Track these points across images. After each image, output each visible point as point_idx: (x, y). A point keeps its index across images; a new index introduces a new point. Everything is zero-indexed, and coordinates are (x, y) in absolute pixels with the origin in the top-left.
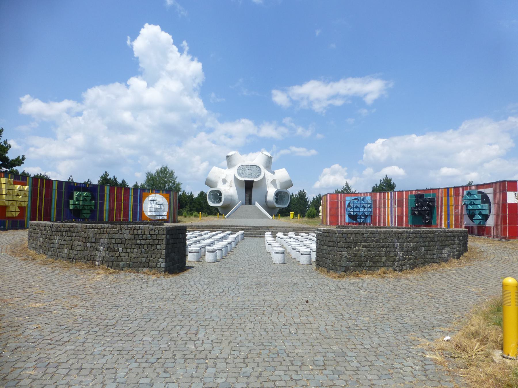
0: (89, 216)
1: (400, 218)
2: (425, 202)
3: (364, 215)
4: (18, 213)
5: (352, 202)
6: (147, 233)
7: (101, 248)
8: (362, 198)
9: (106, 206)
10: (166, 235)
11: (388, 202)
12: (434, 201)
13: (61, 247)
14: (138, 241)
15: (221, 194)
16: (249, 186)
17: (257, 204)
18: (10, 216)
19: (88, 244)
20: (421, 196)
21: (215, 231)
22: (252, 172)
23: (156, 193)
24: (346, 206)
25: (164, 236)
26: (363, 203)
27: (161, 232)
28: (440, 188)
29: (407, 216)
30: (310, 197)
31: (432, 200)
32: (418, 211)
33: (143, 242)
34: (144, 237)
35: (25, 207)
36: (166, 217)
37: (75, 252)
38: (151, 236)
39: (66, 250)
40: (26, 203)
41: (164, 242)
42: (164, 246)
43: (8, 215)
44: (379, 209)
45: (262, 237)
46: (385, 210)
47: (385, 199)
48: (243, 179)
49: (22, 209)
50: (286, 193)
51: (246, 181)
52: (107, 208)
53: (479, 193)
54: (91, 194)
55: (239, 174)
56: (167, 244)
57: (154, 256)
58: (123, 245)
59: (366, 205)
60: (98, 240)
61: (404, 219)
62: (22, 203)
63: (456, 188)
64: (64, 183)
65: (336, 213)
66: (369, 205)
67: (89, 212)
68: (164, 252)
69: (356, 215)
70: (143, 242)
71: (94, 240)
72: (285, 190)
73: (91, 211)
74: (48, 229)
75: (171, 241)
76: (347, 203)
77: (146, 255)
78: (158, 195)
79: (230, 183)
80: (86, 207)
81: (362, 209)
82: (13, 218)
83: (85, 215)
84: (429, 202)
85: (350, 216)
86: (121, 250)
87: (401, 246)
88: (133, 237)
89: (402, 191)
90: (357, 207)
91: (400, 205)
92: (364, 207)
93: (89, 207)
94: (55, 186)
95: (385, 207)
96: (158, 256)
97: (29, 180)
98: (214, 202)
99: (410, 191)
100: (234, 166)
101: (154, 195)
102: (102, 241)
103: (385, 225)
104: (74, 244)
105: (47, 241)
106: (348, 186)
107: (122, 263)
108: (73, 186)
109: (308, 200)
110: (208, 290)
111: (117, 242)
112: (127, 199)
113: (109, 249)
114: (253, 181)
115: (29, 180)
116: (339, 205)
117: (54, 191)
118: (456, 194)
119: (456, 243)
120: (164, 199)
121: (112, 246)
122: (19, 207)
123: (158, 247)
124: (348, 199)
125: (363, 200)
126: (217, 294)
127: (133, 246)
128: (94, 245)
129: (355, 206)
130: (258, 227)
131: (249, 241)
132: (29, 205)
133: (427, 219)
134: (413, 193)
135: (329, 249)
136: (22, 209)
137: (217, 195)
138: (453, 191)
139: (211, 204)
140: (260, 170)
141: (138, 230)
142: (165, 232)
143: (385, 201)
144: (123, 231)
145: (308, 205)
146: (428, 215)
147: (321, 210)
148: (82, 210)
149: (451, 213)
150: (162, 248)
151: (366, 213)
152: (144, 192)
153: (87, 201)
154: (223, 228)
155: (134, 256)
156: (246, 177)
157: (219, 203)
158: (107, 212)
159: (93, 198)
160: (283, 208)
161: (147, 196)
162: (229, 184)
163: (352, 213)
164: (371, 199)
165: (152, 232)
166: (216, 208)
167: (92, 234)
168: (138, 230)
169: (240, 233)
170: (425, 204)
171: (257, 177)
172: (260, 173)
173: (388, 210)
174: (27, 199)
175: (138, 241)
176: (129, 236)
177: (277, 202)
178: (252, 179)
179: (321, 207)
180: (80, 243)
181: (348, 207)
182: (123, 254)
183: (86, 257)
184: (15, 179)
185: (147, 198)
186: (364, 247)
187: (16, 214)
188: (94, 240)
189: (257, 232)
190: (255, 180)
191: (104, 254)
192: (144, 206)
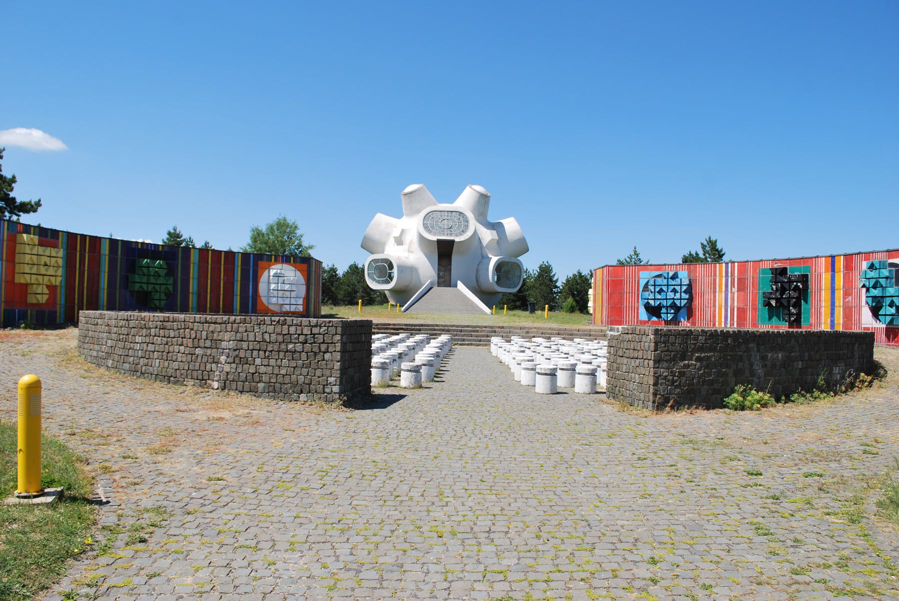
0: (163, 303)
1: (742, 312)
2: (790, 282)
3: (673, 306)
4: (46, 297)
5: (652, 282)
6: (306, 331)
7: (223, 358)
8: (671, 274)
9: (193, 286)
10: (342, 335)
11: (721, 281)
12: (807, 281)
13: (147, 355)
14: (290, 346)
15: (391, 266)
16: (444, 252)
17: (461, 286)
18: (34, 301)
19: (198, 351)
20: (783, 271)
21: (398, 334)
22: (451, 224)
23: (282, 262)
24: (641, 289)
25: (338, 337)
26: (673, 283)
27: (332, 330)
28: (818, 257)
29: (754, 309)
30: (561, 276)
31: (804, 279)
32: (777, 300)
33: (299, 347)
34: (302, 338)
35: (56, 286)
36: (301, 308)
37: (175, 365)
38: (314, 337)
39: (158, 361)
40: (59, 279)
41: (338, 349)
42: (338, 356)
43: (31, 299)
44: (702, 295)
45: (486, 345)
46: (715, 296)
47: (715, 275)
48: (435, 238)
49: (52, 288)
50: (518, 266)
52: (196, 289)
53: (891, 265)
54: (167, 264)
55: (426, 227)
56: (343, 352)
57: (318, 373)
58: (262, 353)
59: (678, 288)
60: (216, 343)
61: (749, 315)
62: (52, 279)
63: (848, 258)
64: (120, 243)
65: (622, 303)
66: (684, 288)
67: (163, 297)
68: (337, 365)
69: (660, 307)
70: (299, 347)
71: (208, 343)
72: (513, 260)
73: (166, 294)
74: (122, 323)
75: (349, 347)
76: (642, 283)
77: (305, 371)
78: (285, 266)
79: (409, 247)
80: (157, 287)
81: (671, 295)
82: (38, 305)
83: (157, 303)
84: (797, 282)
85: (648, 307)
86: (258, 361)
87: (764, 358)
88: (280, 338)
89: (747, 262)
90: (660, 292)
91: (742, 287)
92: (674, 291)
93: (163, 287)
94: (105, 249)
95: (715, 292)
96: (328, 372)
97: (62, 239)
98: (379, 282)
99: (761, 261)
100: (418, 211)
101: (279, 266)
102: (224, 344)
103: (714, 325)
104: (171, 349)
105: (121, 344)
106: (635, 252)
107: (261, 386)
108: (135, 249)
110: (428, 431)
111: (251, 348)
112: (230, 272)
113: (237, 360)
114: (453, 241)
115: (62, 239)
116: (626, 288)
117: (103, 258)
118: (848, 267)
119: (857, 356)
120: (298, 273)
121: (242, 354)
122: (48, 286)
123: (327, 356)
124: (645, 276)
125: (675, 277)
126: (446, 437)
127: (282, 355)
128: (209, 352)
129: (657, 289)
130: (475, 327)
131: (461, 351)
132: (63, 284)
133: (793, 314)
134: (768, 266)
135: (634, 363)
136: (52, 288)
137: (385, 269)
138: (840, 263)
139: (373, 285)
140: (467, 221)
141: (289, 326)
142: (339, 330)
143: (715, 280)
144: (263, 328)
145: (556, 287)
146: (794, 306)
147: (591, 297)
148: (151, 292)
149: (837, 304)
150: (334, 358)
151: (678, 303)
152: (262, 260)
153: (159, 276)
154: (412, 330)
155: (283, 372)
158: (195, 297)
159: (171, 271)
160: (510, 293)
161: (268, 268)
163: (652, 302)
164: (689, 275)
165: (315, 330)
166: (382, 294)
167: (204, 333)
168: (289, 326)
169: (444, 338)
170: (790, 287)
172: (467, 227)
173: (720, 297)
174: (60, 272)
175: (290, 346)
176: (274, 336)
179: (591, 292)
180: (182, 348)
181: (643, 291)
182: (263, 369)
183: (195, 373)
184: (40, 236)
185: (266, 272)
186: (698, 359)
187: (43, 299)
188: (208, 343)
189: (477, 336)
190: (457, 239)
191: (227, 368)
192: (262, 287)
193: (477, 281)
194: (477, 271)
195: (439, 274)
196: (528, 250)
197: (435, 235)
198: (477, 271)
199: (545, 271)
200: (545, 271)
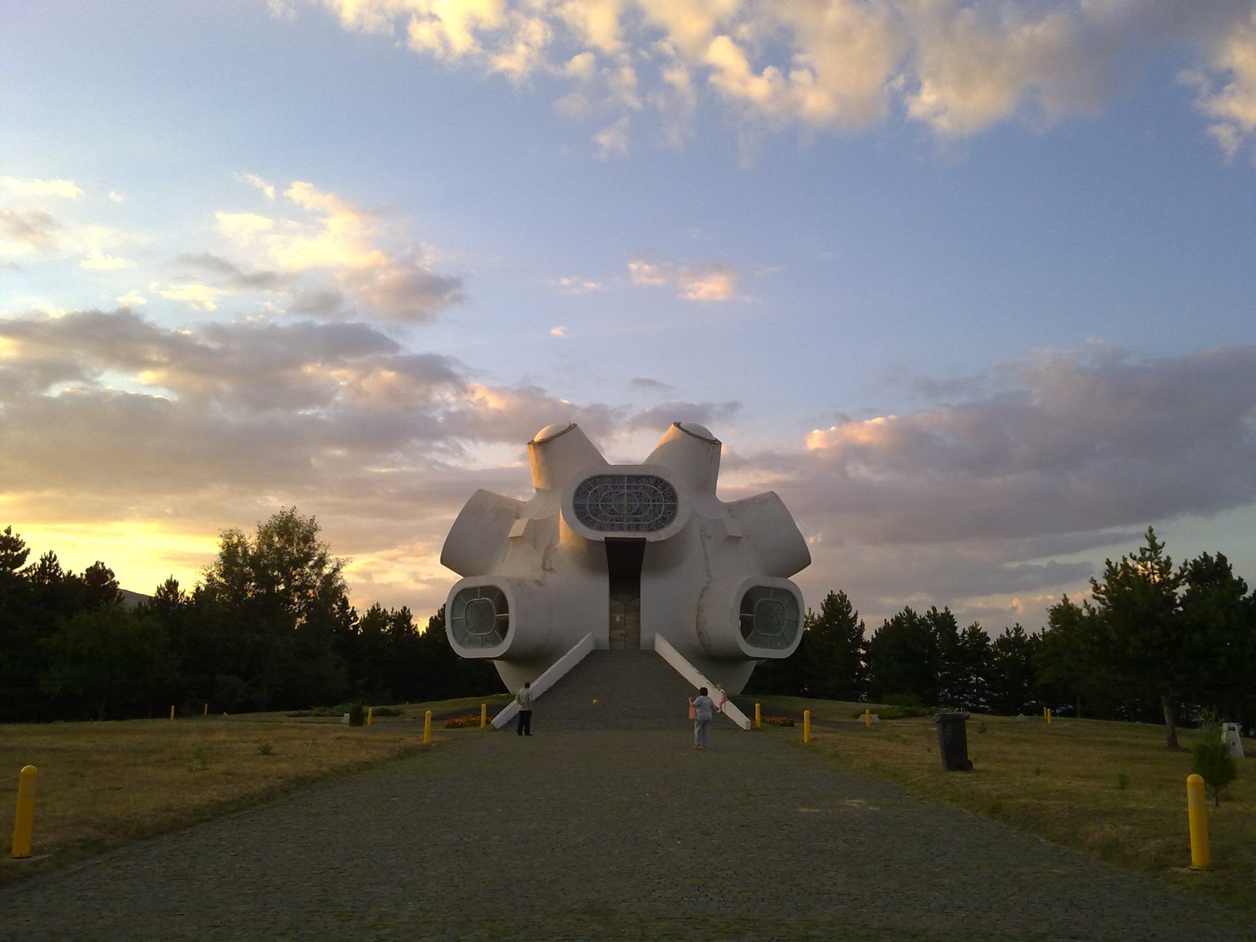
15: (503, 605)
48: (600, 536)
50: (791, 599)
51: (609, 542)
72: (779, 583)
79: (545, 559)
109: (858, 624)
114: (642, 542)
156: (612, 528)
157: (496, 642)
162: (539, 559)
166: (485, 665)
171: (659, 526)
177: (746, 629)
178: (639, 535)
190: (651, 537)
193: (700, 633)
194: (699, 609)
195: (612, 619)
196: (806, 561)
197: (601, 528)
198: (699, 609)
199: (837, 607)
200: (837, 607)
